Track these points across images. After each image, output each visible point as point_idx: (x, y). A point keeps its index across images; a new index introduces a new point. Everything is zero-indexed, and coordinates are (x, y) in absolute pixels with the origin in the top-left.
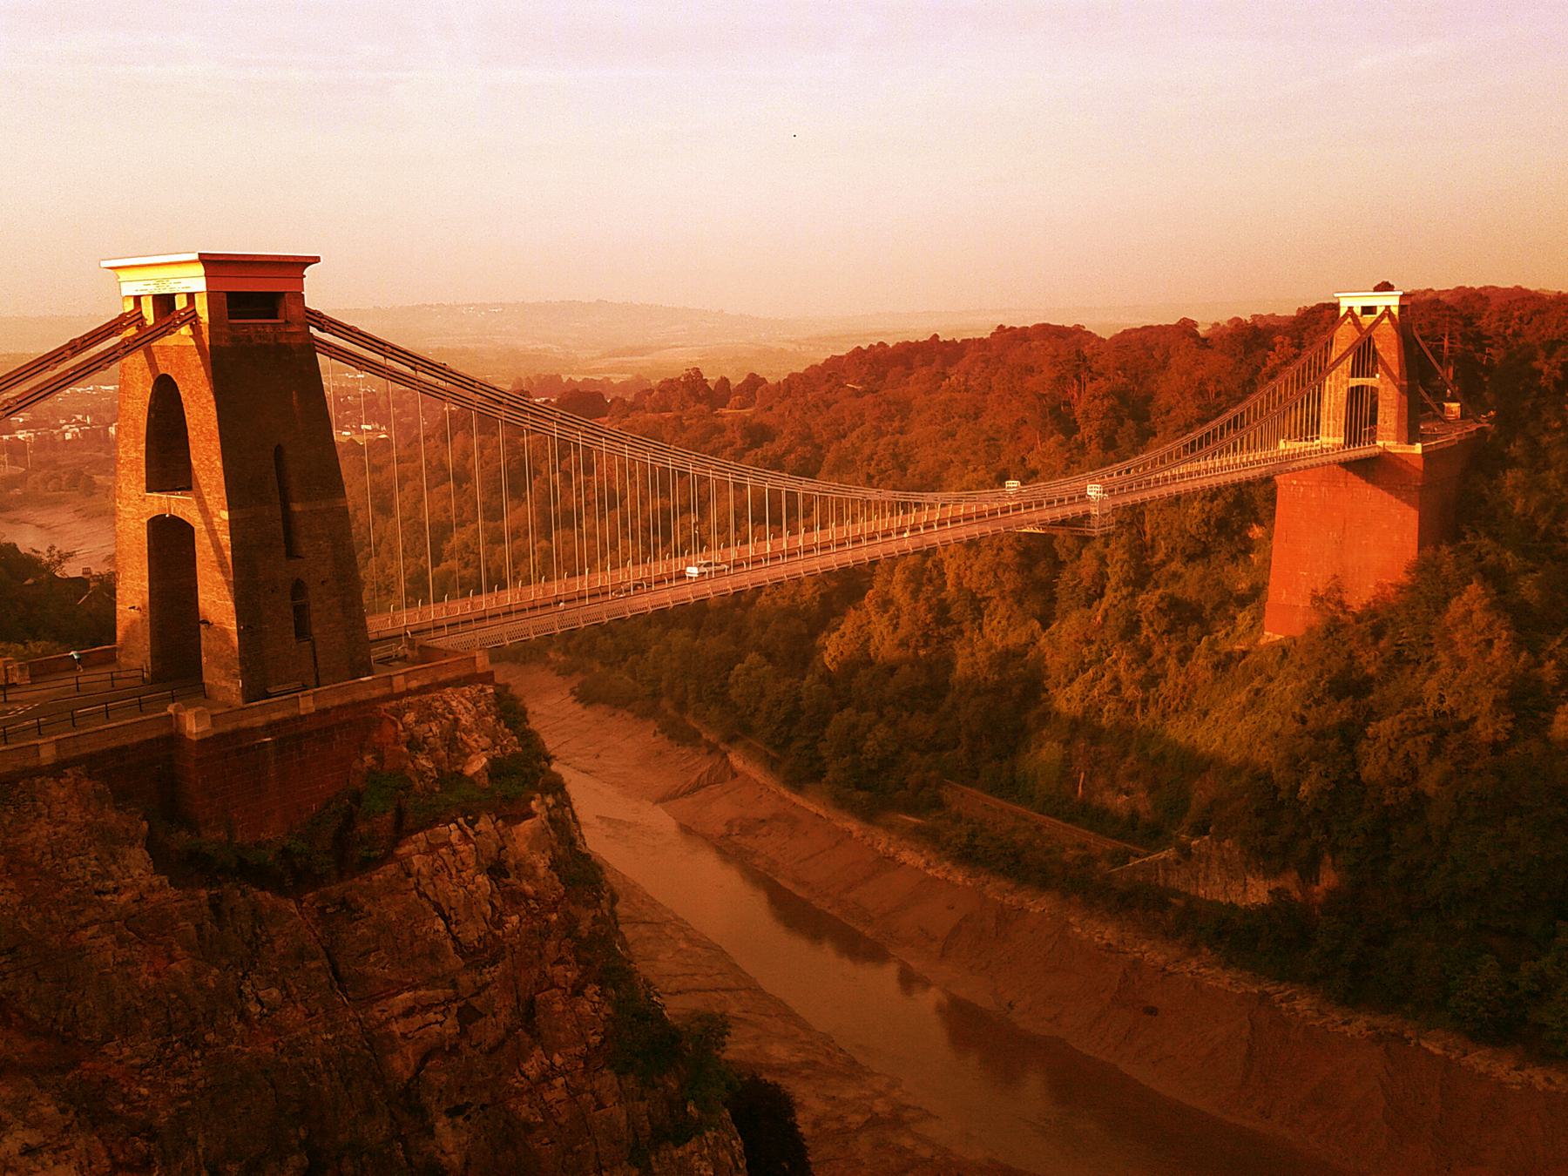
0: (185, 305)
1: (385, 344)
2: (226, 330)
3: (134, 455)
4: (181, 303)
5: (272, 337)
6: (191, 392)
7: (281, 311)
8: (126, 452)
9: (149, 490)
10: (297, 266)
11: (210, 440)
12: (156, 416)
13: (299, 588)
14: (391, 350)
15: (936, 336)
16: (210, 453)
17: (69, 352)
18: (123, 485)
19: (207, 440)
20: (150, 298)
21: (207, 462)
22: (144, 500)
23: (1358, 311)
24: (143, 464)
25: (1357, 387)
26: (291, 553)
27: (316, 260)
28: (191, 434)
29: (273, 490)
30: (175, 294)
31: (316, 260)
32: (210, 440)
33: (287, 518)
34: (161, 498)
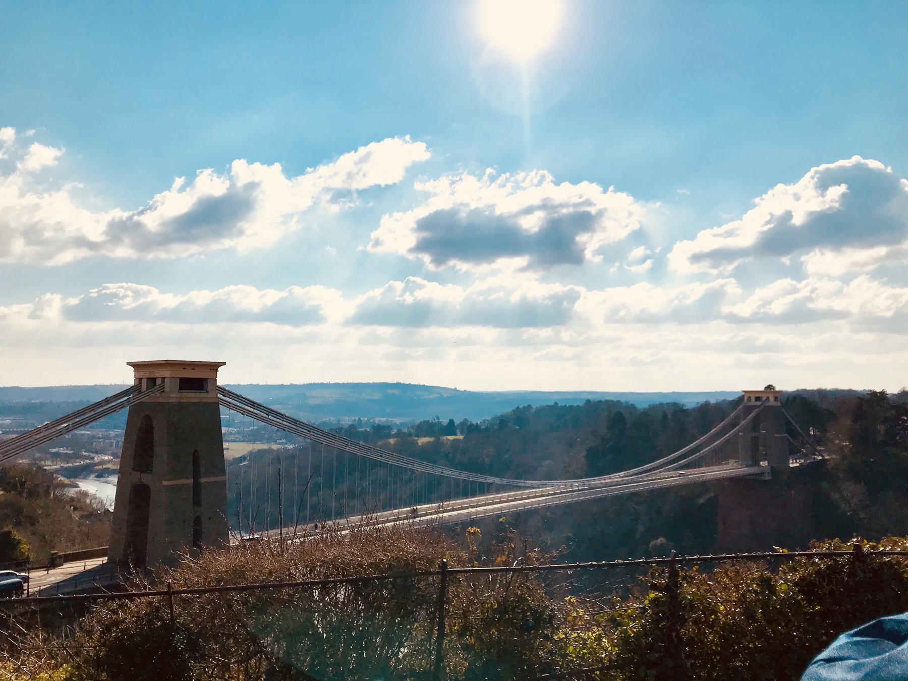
0: (160, 383)
1: (254, 403)
4: (159, 382)
9: (134, 470)
10: (214, 367)
13: (197, 521)
15: (556, 404)
17: (104, 403)
20: (146, 380)
23: (753, 399)
25: (754, 437)
26: (197, 502)
27: (224, 364)
30: (156, 378)
31: (224, 364)
33: (197, 486)
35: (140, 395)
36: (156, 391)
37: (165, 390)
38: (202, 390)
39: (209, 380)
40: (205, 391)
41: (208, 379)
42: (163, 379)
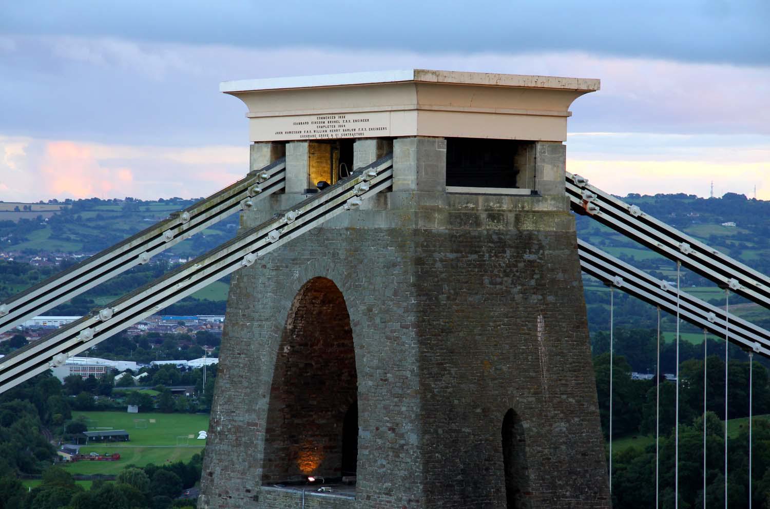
0: (372, 157)
2: (440, 204)
3: (247, 418)
4: (364, 155)
5: (511, 217)
6: (370, 310)
7: (524, 176)
8: (230, 413)
9: (267, 480)
11: (400, 397)
12: (293, 352)
14: (690, 250)
16: (398, 419)
18: (218, 470)
19: (395, 396)
20: (306, 144)
21: (391, 435)
22: (256, 498)
24: (261, 435)
28: (364, 384)
29: (498, 490)
30: (352, 141)
32: (400, 397)
34: (291, 496)
35: (316, 203)
36: (365, 187)
37: (398, 184)
38: (513, 185)
39: (539, 147)
40: (526, 191)
41: (531, 144)
42: (386, 144)
